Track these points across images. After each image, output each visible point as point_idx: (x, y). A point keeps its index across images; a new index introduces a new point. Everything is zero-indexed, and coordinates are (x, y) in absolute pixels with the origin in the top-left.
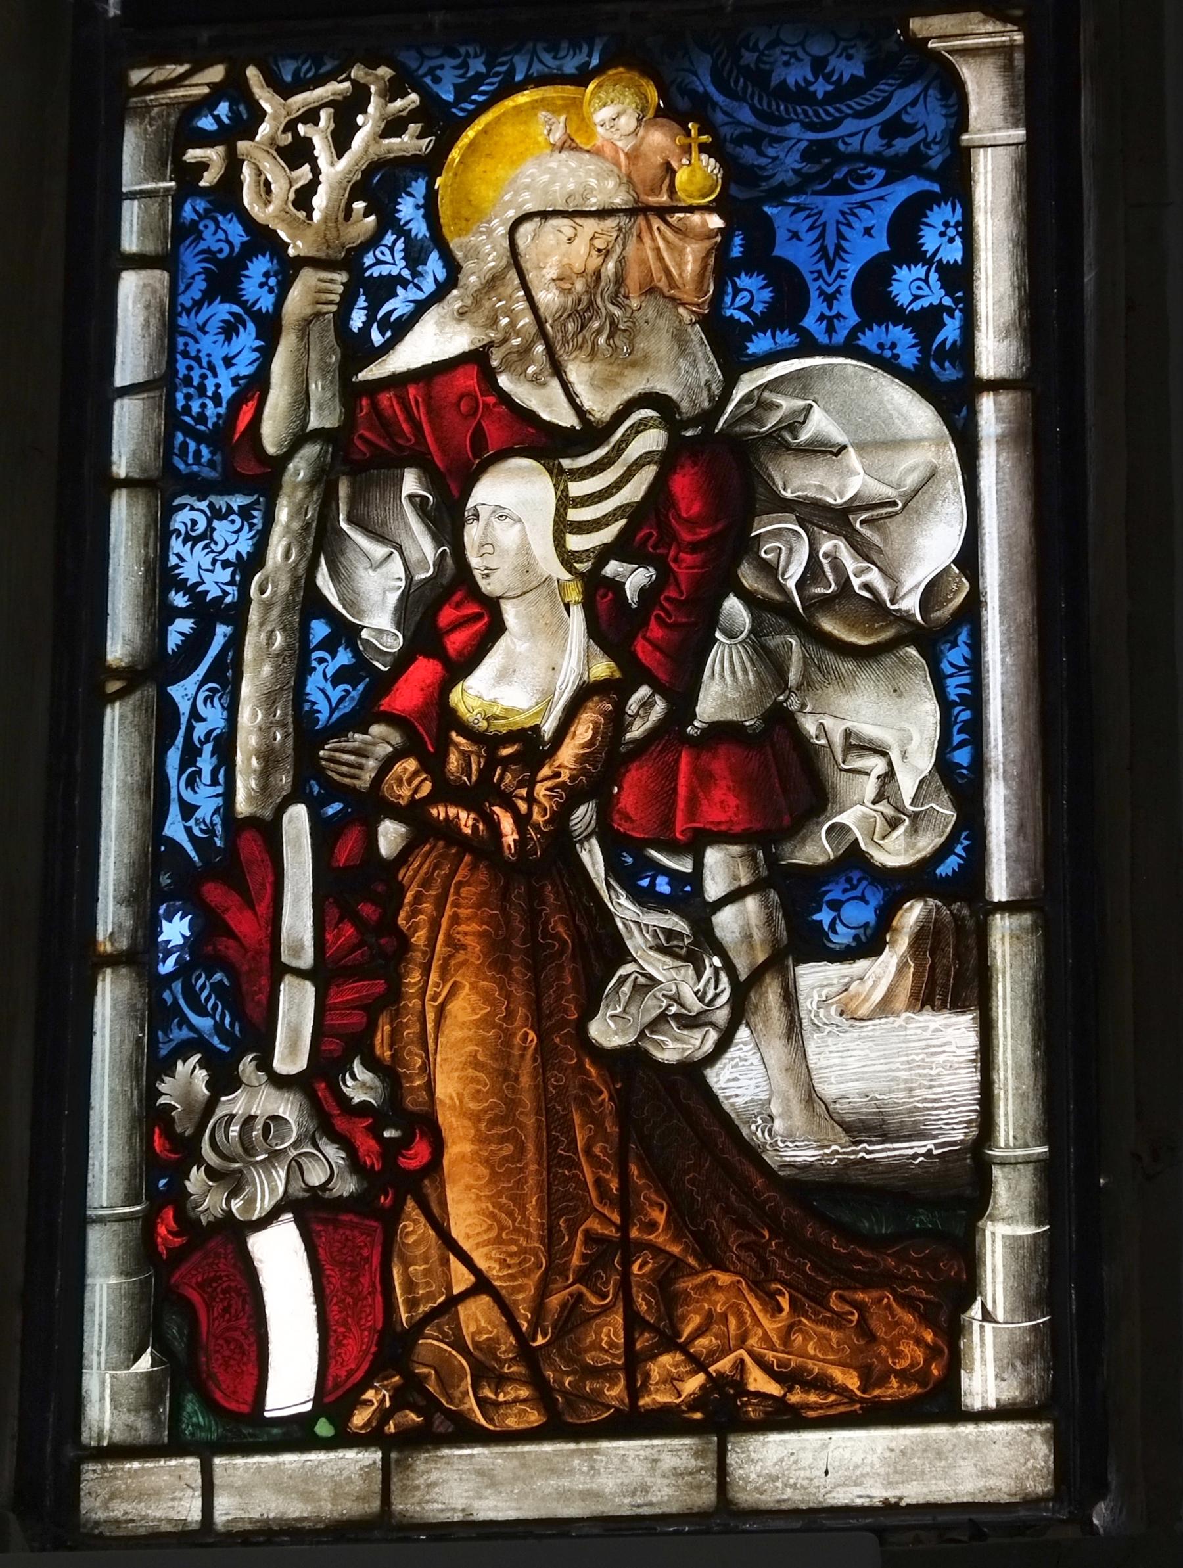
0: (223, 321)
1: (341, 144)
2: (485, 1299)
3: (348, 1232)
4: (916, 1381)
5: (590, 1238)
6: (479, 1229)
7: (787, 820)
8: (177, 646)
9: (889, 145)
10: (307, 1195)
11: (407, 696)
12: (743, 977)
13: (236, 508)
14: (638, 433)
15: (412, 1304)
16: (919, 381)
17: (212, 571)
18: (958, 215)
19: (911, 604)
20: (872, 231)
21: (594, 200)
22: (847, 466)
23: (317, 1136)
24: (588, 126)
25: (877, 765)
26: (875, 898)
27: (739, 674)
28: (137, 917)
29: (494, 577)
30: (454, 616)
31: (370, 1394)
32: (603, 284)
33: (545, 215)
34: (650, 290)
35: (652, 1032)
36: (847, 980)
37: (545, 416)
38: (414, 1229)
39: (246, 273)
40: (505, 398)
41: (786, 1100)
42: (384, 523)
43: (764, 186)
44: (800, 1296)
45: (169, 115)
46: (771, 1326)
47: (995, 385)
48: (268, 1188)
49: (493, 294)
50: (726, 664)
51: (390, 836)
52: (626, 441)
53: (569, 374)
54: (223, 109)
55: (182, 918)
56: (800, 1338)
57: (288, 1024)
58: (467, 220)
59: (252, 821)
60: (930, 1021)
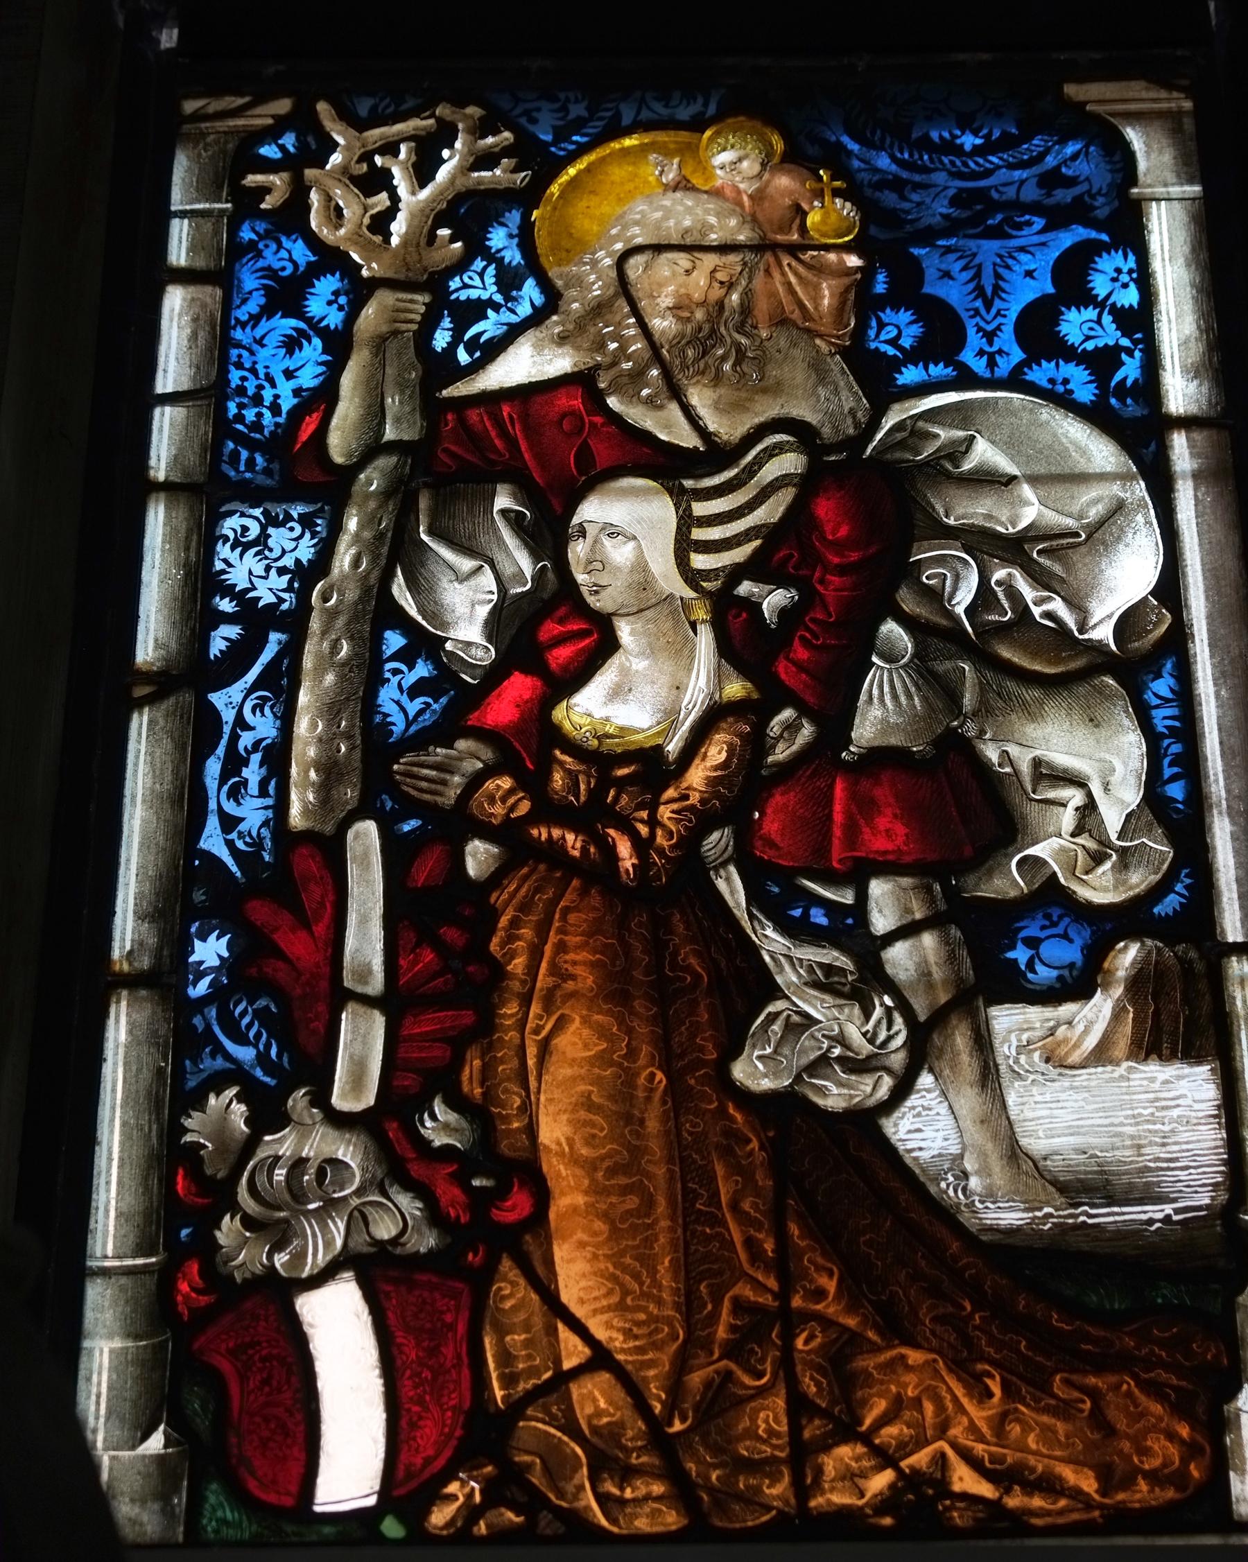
0: (284, 336)
1: (423, 173)
2: (605, 1377)
3: (426, 1294)
4: (1172, 1484)
5: (739, 1306)
6: (596, 1293)
7: (968, 852)
8: (221, 651)
9: (1049, 195)
10: (372, 1250)
11: (502, 709)
12: (922, 1018)
13: (296, 516)
14: (772, 456)
15: (509, 1381)
16: (1097, 415)
17: (266, 578)
18: (1131, 263)
19: (1104, 633)
20: (1035, 274)
21: (713, 236)
22: (1019, 496)
23: (387, 1183)
24: (705, 168)
25: (1075, 797)
26: (1081, 936)
27: (903, 699)
28: (163, 935)
29: (604, 594)
30: (556, 631)
31: (453, 1487)
32: (726, 314)
33: (658, 249)
34: (781, 321)
35: (811, 1076)
36: (1052, 1023)
37: (663, 437)
38: (512, 1291)
39: (312, 290)
40: (616, 419)
41: (983, 1156)
42: (472, 537)
43: (908, 228)
44: (1014, 1379)
45: (226, 142)
46: (979, 1414)
47: (1186, 423)
48: (323, 1241)
49: (598, 320)
50: (886, 689)
51: (478, 857)
52: (759, 463)
53: (690, 397)
54: (289, 140)
55: (218, 938)
56: (1018, 1429)
57: (351, 1057)
58: (568, 251)
59: (307, 836)
60: (1156, 1072)
